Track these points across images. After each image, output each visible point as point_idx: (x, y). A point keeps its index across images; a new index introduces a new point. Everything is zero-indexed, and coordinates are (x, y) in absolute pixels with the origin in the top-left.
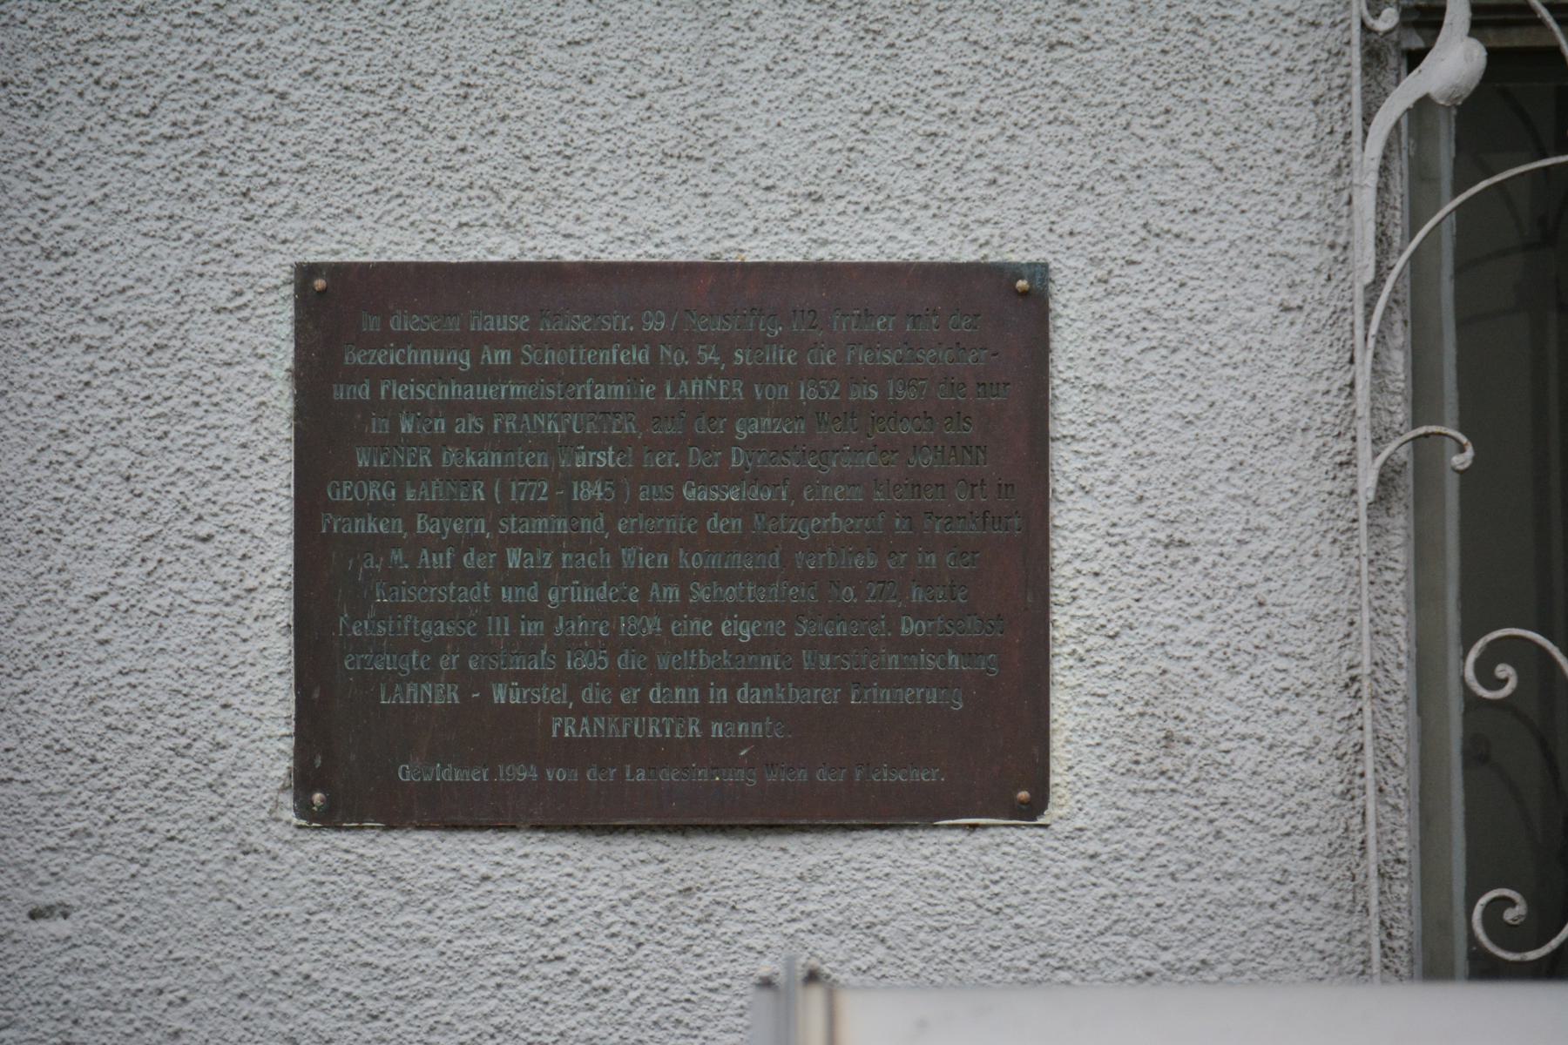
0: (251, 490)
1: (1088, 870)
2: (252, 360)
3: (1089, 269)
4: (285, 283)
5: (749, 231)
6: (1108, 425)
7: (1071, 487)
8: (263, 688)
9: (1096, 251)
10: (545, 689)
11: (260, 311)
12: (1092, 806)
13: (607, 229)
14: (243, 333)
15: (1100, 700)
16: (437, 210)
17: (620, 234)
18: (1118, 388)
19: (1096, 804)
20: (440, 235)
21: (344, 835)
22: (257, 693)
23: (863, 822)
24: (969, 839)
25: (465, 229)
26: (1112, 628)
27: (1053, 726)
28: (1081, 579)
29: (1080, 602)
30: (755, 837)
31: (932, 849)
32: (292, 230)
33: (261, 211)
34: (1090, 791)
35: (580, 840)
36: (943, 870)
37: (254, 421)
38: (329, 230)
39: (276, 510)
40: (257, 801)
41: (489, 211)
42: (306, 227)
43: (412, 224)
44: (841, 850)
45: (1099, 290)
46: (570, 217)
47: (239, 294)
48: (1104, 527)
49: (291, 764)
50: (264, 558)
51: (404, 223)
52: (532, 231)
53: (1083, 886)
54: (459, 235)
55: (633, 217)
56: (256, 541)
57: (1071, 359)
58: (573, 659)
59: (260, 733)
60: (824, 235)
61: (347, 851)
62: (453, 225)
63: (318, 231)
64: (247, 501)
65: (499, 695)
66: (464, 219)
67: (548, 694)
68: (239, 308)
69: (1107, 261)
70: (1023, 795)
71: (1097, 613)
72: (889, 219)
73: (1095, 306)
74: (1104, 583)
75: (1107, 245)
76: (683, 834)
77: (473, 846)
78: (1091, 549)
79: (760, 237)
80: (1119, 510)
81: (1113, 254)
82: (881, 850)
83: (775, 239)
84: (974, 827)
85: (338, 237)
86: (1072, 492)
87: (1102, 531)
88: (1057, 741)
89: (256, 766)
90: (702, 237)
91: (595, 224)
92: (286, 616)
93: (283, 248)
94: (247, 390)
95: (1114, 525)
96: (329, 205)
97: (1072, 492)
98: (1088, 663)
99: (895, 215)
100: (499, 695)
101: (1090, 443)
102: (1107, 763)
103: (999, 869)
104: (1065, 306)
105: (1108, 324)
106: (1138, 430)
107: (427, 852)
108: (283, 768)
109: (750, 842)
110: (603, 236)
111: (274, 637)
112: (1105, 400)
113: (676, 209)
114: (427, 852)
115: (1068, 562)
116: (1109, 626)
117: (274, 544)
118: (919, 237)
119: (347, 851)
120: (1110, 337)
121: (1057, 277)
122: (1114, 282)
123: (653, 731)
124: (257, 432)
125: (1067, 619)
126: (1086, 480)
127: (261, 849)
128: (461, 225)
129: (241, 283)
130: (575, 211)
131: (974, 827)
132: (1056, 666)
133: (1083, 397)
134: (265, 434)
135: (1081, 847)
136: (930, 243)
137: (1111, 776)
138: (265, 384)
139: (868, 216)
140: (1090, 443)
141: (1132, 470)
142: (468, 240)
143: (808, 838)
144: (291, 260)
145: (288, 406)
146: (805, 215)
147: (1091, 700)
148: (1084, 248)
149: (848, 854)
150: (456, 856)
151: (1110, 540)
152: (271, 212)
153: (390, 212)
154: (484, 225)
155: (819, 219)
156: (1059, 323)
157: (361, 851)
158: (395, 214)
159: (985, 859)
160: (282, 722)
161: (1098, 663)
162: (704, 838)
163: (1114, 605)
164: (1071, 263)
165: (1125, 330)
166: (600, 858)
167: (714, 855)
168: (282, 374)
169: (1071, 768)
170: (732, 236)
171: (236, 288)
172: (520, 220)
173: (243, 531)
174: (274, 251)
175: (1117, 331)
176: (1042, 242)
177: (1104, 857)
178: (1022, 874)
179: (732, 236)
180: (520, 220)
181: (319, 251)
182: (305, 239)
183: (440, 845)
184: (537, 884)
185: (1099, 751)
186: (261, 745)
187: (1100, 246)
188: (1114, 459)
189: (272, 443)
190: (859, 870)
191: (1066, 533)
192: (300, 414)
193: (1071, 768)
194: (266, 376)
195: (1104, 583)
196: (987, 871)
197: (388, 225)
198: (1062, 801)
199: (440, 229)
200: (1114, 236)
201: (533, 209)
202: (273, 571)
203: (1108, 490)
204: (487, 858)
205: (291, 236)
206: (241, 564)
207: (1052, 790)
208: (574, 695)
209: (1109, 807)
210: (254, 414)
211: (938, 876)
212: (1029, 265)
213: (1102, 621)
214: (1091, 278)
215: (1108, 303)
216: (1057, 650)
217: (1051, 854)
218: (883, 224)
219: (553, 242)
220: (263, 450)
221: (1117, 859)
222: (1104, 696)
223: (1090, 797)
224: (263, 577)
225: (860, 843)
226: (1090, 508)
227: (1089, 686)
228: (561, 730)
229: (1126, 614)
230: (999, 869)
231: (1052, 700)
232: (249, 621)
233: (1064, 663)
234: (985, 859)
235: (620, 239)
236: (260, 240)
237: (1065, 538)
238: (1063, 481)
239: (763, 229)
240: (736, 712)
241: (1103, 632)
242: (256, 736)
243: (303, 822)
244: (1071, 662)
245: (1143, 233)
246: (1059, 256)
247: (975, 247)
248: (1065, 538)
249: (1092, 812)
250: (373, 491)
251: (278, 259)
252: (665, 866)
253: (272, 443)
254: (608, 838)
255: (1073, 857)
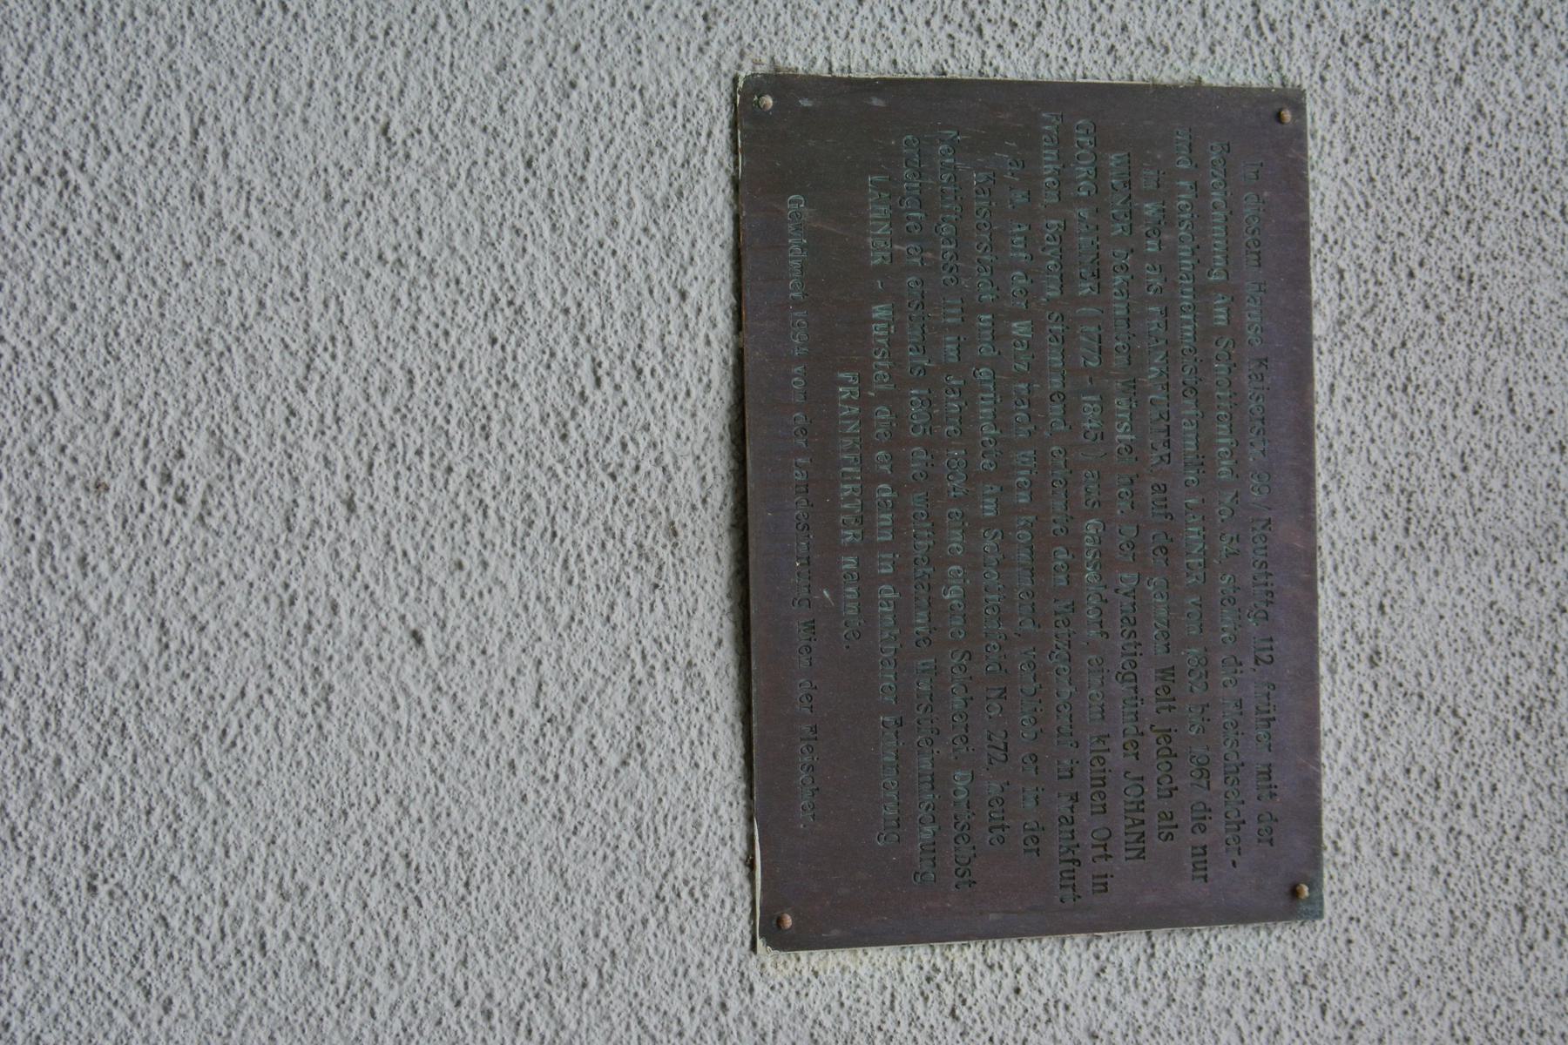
0: (1081, 35)
1: (708, 1001)
2: (1208, 40)
3: (1315, 962)
4: (1283, 78)
5: (1341, 588)
6: (1165, 995)
7: (1103, 957)
8: (880, 44)
9: (1333, 971)
10: (887, 364)
11: (1256, 50)
12: (776, 1001)
13: (1339, 432)
14: (1234, 31)
15: (888, 1003)
16: (1355, 246)
17: (1336, 447)
18: (1203, 1003)
19: (779, 1007)
20: (1331, 249)
21: (727, 131)
22: (874, 36)
23: (755, 735)
24: (736, 858)
25: (1337, 277)
26: (962, 1012)
27: (860, 951)
28: (1011, 974)
29: (987, 973)
30: (732, 610)
31: (725, 818)
32: (1334, 87)
33: (1351, 54)
34: (792, 997)
35: (726, 406)
36: (703, 831)
37: (1149, 40)
38: (1335, 128)
39: (1061, 61)
40: (762, 31)
41: (1354, 303)
42: (1338, 102)
43: (1341, 219)
44: (722, 711)
45: (1296, 976)
46: (1350, 392)
47: (1272, 29)
48: (1064, 996)
49: (801, 72)
50: (1013, 47)
51: (1342, 211)
52: (1336, 349)
53: (690, 998)
54: (1332, 270)
55: (1352, 459)
56: (1029, 39)
57: (1229, 949)
58: (919, 396)
59: (833, 37)
60: (1340, 670)
61: (709, 134)
62: (1342, 265)
63: (1334, 116)
64: (1069, 30)
65: (880, 311)
66: (1347, 275)
67: (883, 368)
68: (1259, 27)
69: (1324, 983)
70: (788, 921)
71: (977, 994)
72: (1356, 739)
73: (1280, 972)
74: (1008, 1000)
75: (1339, 981)
76: (733, 526)
77: (718, 281)
78: (1042, 983)
79: (1336, 599)
80: (1080, 1012)
81: (1331, 989)
82: (722, 757)
83: (1335, 617)
84: (751, 865)
85: (1328, 137)
86: (1097, 958)
87: (1060, 995)
88: (843, 956)
89: (799, 32)
90: (1335, 536)
91: (1343, 419)
92: (954, 71)
93: (1316, 78)
94: (1179, 33)
95: (1067, 1008)
96: (1358, 130)
97: (1097, 958)
98: (926, 987)
99: (1361, 747)
100: (880, 311)
101: (1146, 975)
102: (823, 1017)
103: (706, 896)
104: (1279, 938)
105: (1264, 988)
106: (1162, 1027)
107: (710, 227)
108: (795, 62)
109: (727, 604)
110: (1332, 426)
111: (933, 56)
112: (1190, 989)
113: (1360, 507)
114: (710, 227)
115: (1028, 958)
116: (964, 1009)
117: (1026, 58)
118: (1341, 775)
119: (709, 134)
120: (1251, 991)
121: (1306, 930)
122: (1305, 991)
123: (847, 489)
124: (1138, 43)
125: (970, 960)
126: (1111, 973)
127: (711, 35)
128: (1341, 272)
129: (1283, 30)
130: (1355, 397)
131: (751, 865)
132: (921, 950)
133: (1192, 965)
134: (1137, 52)
135: (732, 992)
136: (1336, 787)
137: (809, 1022)
138: (1185, 54)
139: (1359, 717)
140: (1146, 975)
141: (1122, 1025)
142: (1327, 280)
143: (733, 671)
144: (1305, 86)
145: (1165, 77)
146: (1358, 648)
147: (887, 994)
148: (1335, 956)
149: (717, 719)
150: (707, 261)
151: (1051, 1004)
152: (1350, 64)
153: (1352, 194)
154: (1341, 297)
155: (1355, 664)
156: (1263, 933)
157: (710, 150)
158: (1350, 200)
159: (717, 879)
160: (845, 63)
161: (926, 999)
162: (730, 550)
163: (985, 1013)
164: (1321, 943)
165: (1259, 1008)
166: (706, 429)
167: (712, 562)
168: (1195, 74)
169: (816, 974)
170: (1335, 569)
171: (1278, 25)
172: (1347, 337)
173: (1039, 24)
174: (1313, 67)
175: (1257, 998)
176: (1340, 910)
177: (722, 1019)
178: (702, 924)
179: (1335, 569)
180: (1347, 337)
181: (1317, 117)
182: (1325, 102)
183: (718, 242)
184: (678, 355)
185: (835, 1005)
186: (820, 39)
187: (1337, 974)
188: (1132, 1003)
189: (1128, 60)
190: (700, 732)
191: (1056, 954)
192: (1161, 90)
193: (816, 974)
194: (1193, 54)
195: (1008, 1000)
196: (704, 884)
197: (1339, 192)
198: (781, 967)
199: (1337, 249)
200: (1348, 989)
201: (1356, 351)
202: (999, 58)
203: (1101, 999)
204: (705, 297)
205: (1328, 85)
206: (1006, 21)
207: (792, 954)
208: (883, 397)
209: (776, 1021)
210: (1156, 41)
211: (697, 825)
212: (1321, 897)
213: (970, 1002)
214: (1308, 967)
215: (1283, 985)
216: (938, 951)
217: (724, 957)
218: (1351, 733)
219: (1326, 373)
220: (1121, 49)
221: (720, 1035)
222: (892, 1009)
223: (787, 999)
224: (993, 44)
225: (729, 732)
226: (1083, 979)
227: (901, 989)
228: (845, 383)
229: (978, 1027)
230: (706, 896)
231: (886, 948)
232: (948, 29)
233: (925, 959)
234: (717, 879)
235: (1331, 446)
236: (1323, 52)
237: (1051, 952)
238: (1109, 946)
239: (1344, 602)
240: (867, 580)
241: (958, 1002)
242: (830, 32)
243: (741, 84)
244: (927, 967)
245: (1352, 1021)
246: (1327, 930)
247: (1333, 836)
248: (1051, 952)
249: (769, 1002)
250: (1083, 170)
251: (1306, 71)
252: (699, 506)
253: (1128, 60)
254: (727, 439)
255: (722, 984)
